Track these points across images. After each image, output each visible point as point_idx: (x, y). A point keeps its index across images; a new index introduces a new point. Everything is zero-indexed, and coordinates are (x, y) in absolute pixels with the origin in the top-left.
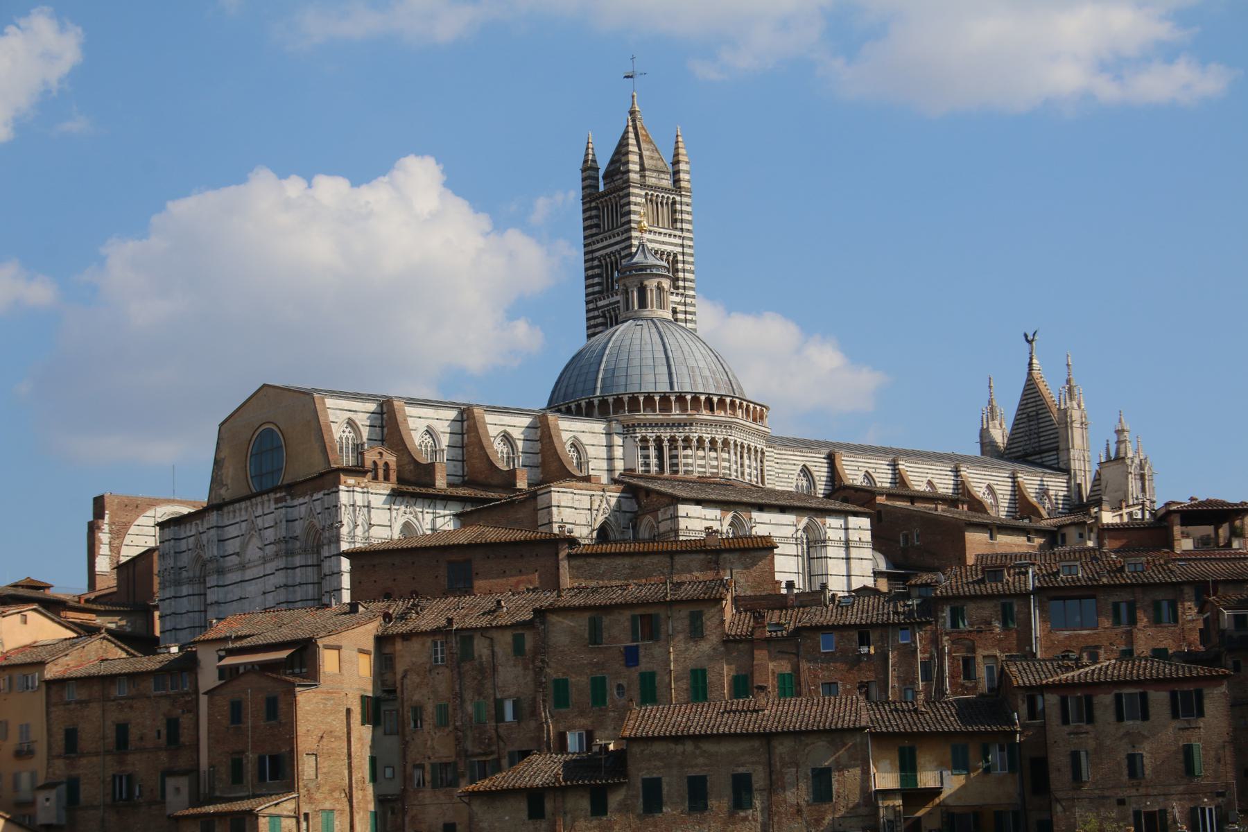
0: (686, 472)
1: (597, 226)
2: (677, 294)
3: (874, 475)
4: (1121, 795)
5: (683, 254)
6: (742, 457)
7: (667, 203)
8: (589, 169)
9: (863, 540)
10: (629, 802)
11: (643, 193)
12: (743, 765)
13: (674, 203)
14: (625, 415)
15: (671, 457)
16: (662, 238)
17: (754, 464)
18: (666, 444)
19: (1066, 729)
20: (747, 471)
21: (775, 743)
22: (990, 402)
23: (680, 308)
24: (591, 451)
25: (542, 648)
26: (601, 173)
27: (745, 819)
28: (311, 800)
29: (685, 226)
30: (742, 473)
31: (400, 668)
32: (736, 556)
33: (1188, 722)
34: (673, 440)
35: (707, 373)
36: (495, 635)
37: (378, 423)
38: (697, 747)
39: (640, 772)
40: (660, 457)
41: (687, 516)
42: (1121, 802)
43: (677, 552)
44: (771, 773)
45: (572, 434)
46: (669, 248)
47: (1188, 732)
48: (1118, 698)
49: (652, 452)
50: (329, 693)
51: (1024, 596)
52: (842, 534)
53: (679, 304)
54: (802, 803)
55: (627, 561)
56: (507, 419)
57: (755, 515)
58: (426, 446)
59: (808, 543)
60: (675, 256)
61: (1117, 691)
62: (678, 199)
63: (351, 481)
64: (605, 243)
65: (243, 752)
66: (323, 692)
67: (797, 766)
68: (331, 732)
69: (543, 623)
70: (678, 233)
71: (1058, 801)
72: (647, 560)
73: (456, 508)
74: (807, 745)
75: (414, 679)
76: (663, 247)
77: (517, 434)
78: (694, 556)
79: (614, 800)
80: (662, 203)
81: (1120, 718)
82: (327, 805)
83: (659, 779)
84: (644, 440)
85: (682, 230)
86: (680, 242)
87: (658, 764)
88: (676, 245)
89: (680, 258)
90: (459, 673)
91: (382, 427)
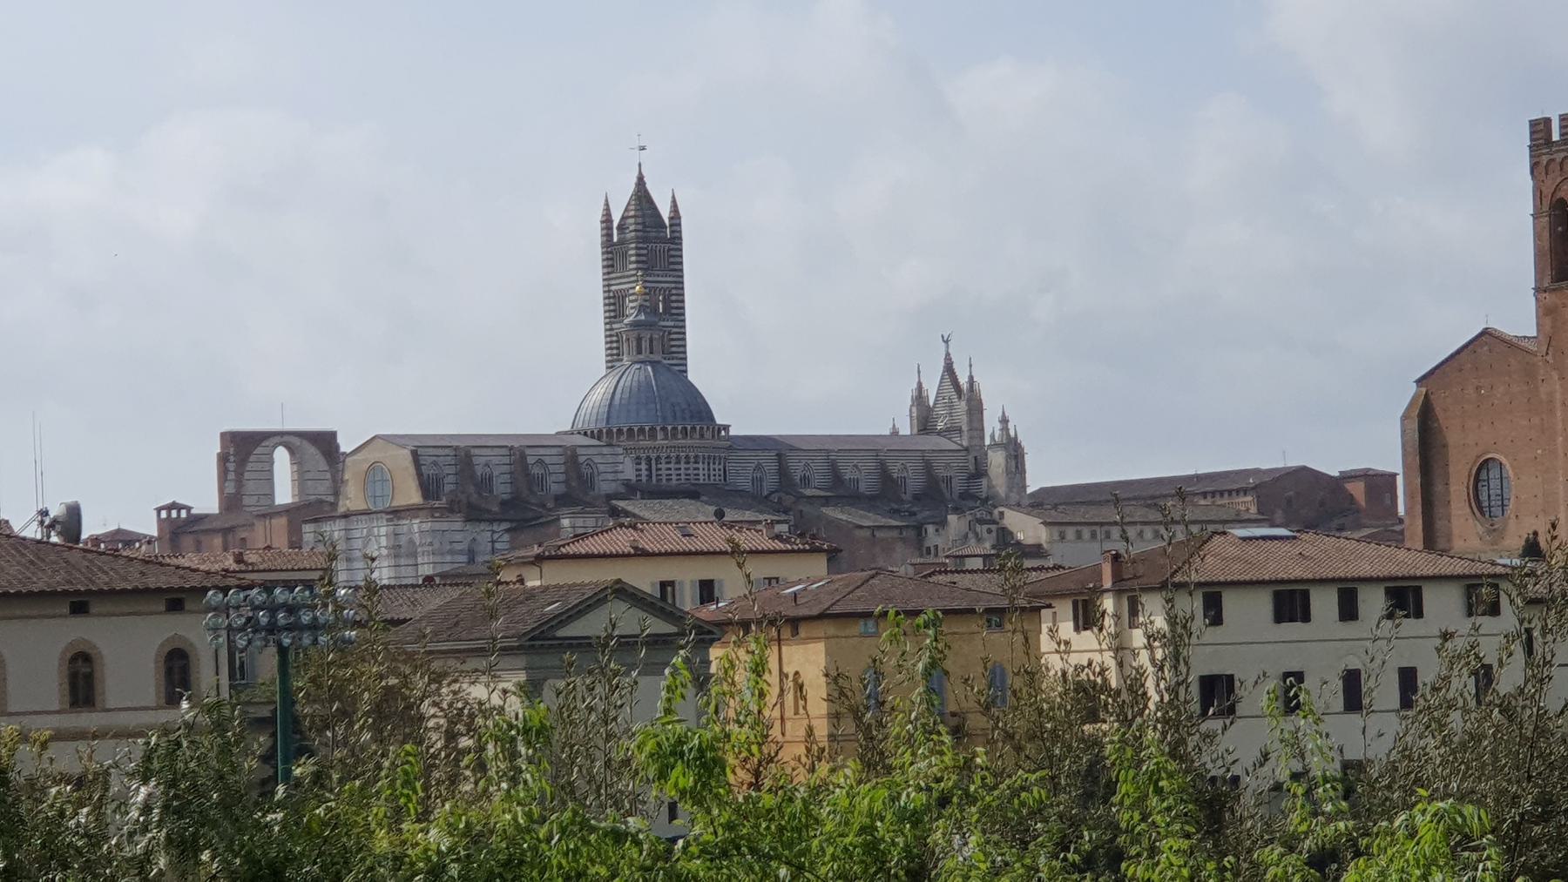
0: (667, 480)
1: (612, 266)
5: (676, 288)
6: (709, 464)
8: (607, 220)
13: (669, 250)
15: (658, 470)
16: (660, 279)
17: (716, 467)
18: (653, 462)
20: (712, 473)
26: (615, 224)
29: (676, 267)
34: (658, 458)
35: (684, 406)
40: (649, 469)
45: (586, 457)
49: (643, 466)
63: (437, 515)
64: (618, 281)
73: (505, 526)
84: (638, 458)
85: (676, 270)
91: (456, 465)
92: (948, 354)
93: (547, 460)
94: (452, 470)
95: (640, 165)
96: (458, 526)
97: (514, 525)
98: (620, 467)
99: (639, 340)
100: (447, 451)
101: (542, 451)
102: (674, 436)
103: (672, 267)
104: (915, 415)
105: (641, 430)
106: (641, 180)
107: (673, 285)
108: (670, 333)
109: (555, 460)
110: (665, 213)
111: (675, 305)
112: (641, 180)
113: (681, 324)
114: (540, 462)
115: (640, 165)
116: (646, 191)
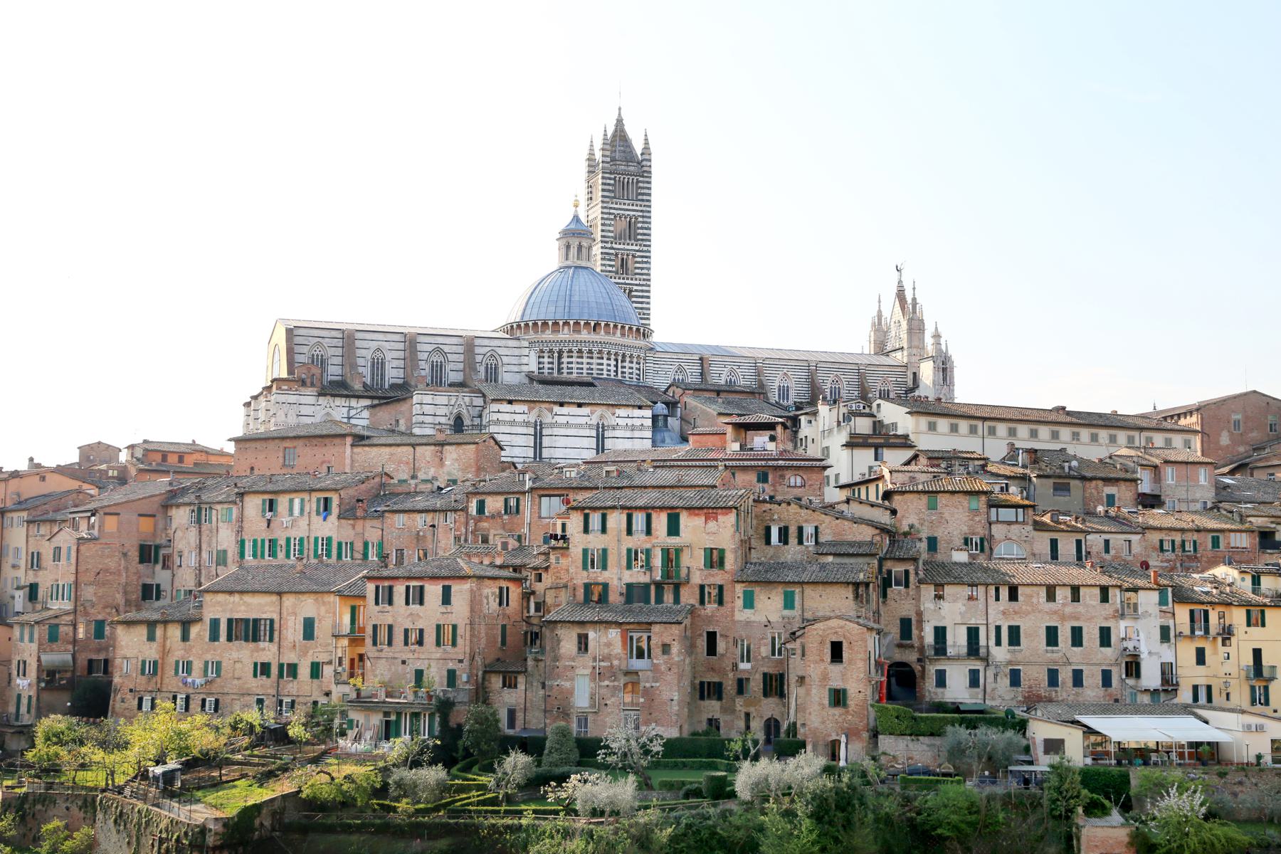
0: (568, 373)
2: (636, 245)
3: (738, 370)
4: (404, 658)
5: (643, 217)
6: (616, 360)
7: (633, 182)
9: (645, 424)
10: (202, 633)
11: (613, 176)
12: (266, 613)
13: (638, 182)
14: (532, 335)
15: (560, 363)
19: (377, 608)
21: (285, 598)
22: (880, 312)
23: (638, 254)
25: (241, 519)
27: (264, 649)
28: (86, 614)
29: (645, 197)
30: (616, 371)
31: (174, 526)
32: (453, 447)
33: (446, 608)
36: (219, 507)
37: (340, 344)
38: (241, 599)
39: (208, 615)
41: (499, 412)
42: (404, 662)
43: (417, 445)
44: (281, 618)
45: (490, 349)
46: (632, 213)
47: (445, 616)
48: (408, 588)
50: (106, 544)
51: (524, 493)
53: (637, 251)
54: (297, 641)
55: (387, 450)
57: (557, 409)
58: (378, 359)
59: (603, 428)
60: (636, 218)
61: (407, 584)
63: (286, 387)
65: (57, 581)
66: (101, 544)
67: (295, 614)
68: (107, 570)
69: (242, 501)
70: (639, 203)
71: (368, 658)
72: (400, 449)
73: (368, 402)
74: (302, 601)
75: (179, 534)
78: (428, 447)
79: (194, 630)
80: (628, 182)
81: (407, 603)
82: (100, 617)
83: (219, 619)
84: (542, 351)
85: (643, 200)
87: (220, 609)
88: (637, 211)
90: (200, 531)
92: (900, 282)
93: (446, 349)
94: (339, 352)
95: (620, 109)
96: (312, 400)
97: (376, 402)
98: (525, 360)
99: (568, 247)
100: (334, 334)
101: (440, 340)
102: (579, 332)
103: (640, 197)
104: (872, 339)
105: (545, 324)
106: (620, 122)
107: (641, 214)
108: (634, 256)
109: (454, 349)
110: (638, 148)
111: (641, 231)
112: (620, 122)
113: (645, 248)
114: (438, 350)
115: (620, 109)
116: (623, 131)
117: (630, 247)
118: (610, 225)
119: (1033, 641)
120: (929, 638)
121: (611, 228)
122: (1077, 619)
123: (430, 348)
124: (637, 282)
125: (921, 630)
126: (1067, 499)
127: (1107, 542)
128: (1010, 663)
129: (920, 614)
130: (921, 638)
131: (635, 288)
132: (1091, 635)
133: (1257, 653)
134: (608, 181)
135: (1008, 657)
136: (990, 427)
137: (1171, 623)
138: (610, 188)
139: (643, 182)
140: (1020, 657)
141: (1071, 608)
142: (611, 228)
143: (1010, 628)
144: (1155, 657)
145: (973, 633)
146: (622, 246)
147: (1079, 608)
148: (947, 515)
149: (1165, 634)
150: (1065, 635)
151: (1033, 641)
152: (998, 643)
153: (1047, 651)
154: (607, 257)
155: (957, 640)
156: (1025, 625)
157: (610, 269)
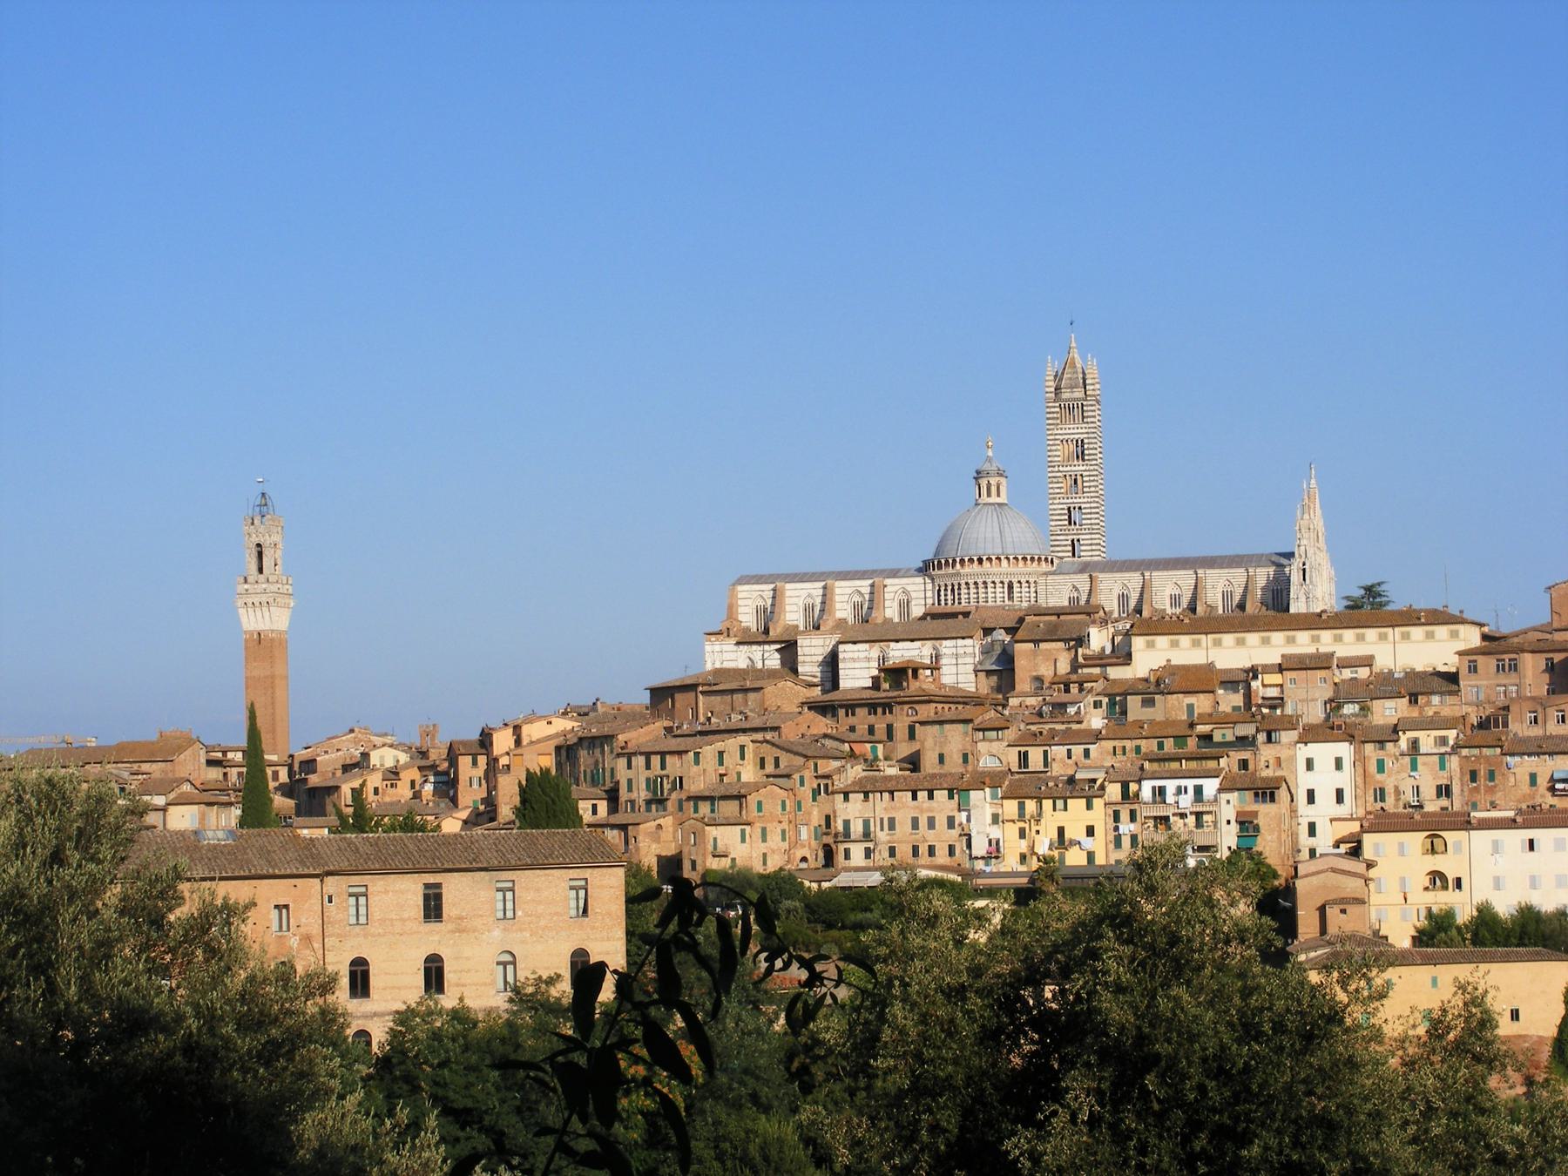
11: (1057, 404)
16: (1072, 431)
23: (1085, 474)
24: (914, 595)
29: (1089, 420)
46: (1076, 437)
52: (954, 650)
53: (1085, 471)
56: (858, 583)
57: (892, 645)
62: (1085, 403)
63: (713, 639)
76: (1072, 437)
77: (863, 590)
86: (1084, 431)
89: (1086, 441)
107: (1086, 436)
117: (1077, 468)
118: (1056, 451)
119: (903, 827)
120: (840, 828)
121: (1057, 453)
122: (932, 811)
123: (849, 591)
124: (1086, 500)
125: (836, 822)
126: (1151, 710)
127: (1069, 751)
128: (889, 842)
129: (835, 812)
130: (836, 827)
131: (1083, 506)
132: (941, 822)
133: (1061, 831)
134: (1053, 410)
135: (888, 838)
136: (1214, 640)
137: (1000, 812)
138: (1055, 415)
139: (1087, 405)
140: (895, 837)
141: (928, 804)
142: (1057, 453)
143: (889, 818)
144: (982, 835)
145: (866, 823)
146: (1069, 468)
147: (933, 804)
148: (949, 738)
149: (996, 819)
150: (923, 822)
151: (903, 827)
152: (882, 829)
153: (912, 834)
154: (1055, 480)
155: (857, 829)
156: (898, 816)
157: (1058, 491)
